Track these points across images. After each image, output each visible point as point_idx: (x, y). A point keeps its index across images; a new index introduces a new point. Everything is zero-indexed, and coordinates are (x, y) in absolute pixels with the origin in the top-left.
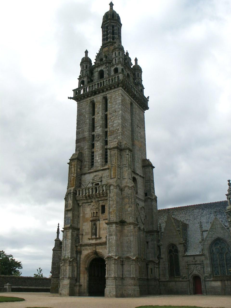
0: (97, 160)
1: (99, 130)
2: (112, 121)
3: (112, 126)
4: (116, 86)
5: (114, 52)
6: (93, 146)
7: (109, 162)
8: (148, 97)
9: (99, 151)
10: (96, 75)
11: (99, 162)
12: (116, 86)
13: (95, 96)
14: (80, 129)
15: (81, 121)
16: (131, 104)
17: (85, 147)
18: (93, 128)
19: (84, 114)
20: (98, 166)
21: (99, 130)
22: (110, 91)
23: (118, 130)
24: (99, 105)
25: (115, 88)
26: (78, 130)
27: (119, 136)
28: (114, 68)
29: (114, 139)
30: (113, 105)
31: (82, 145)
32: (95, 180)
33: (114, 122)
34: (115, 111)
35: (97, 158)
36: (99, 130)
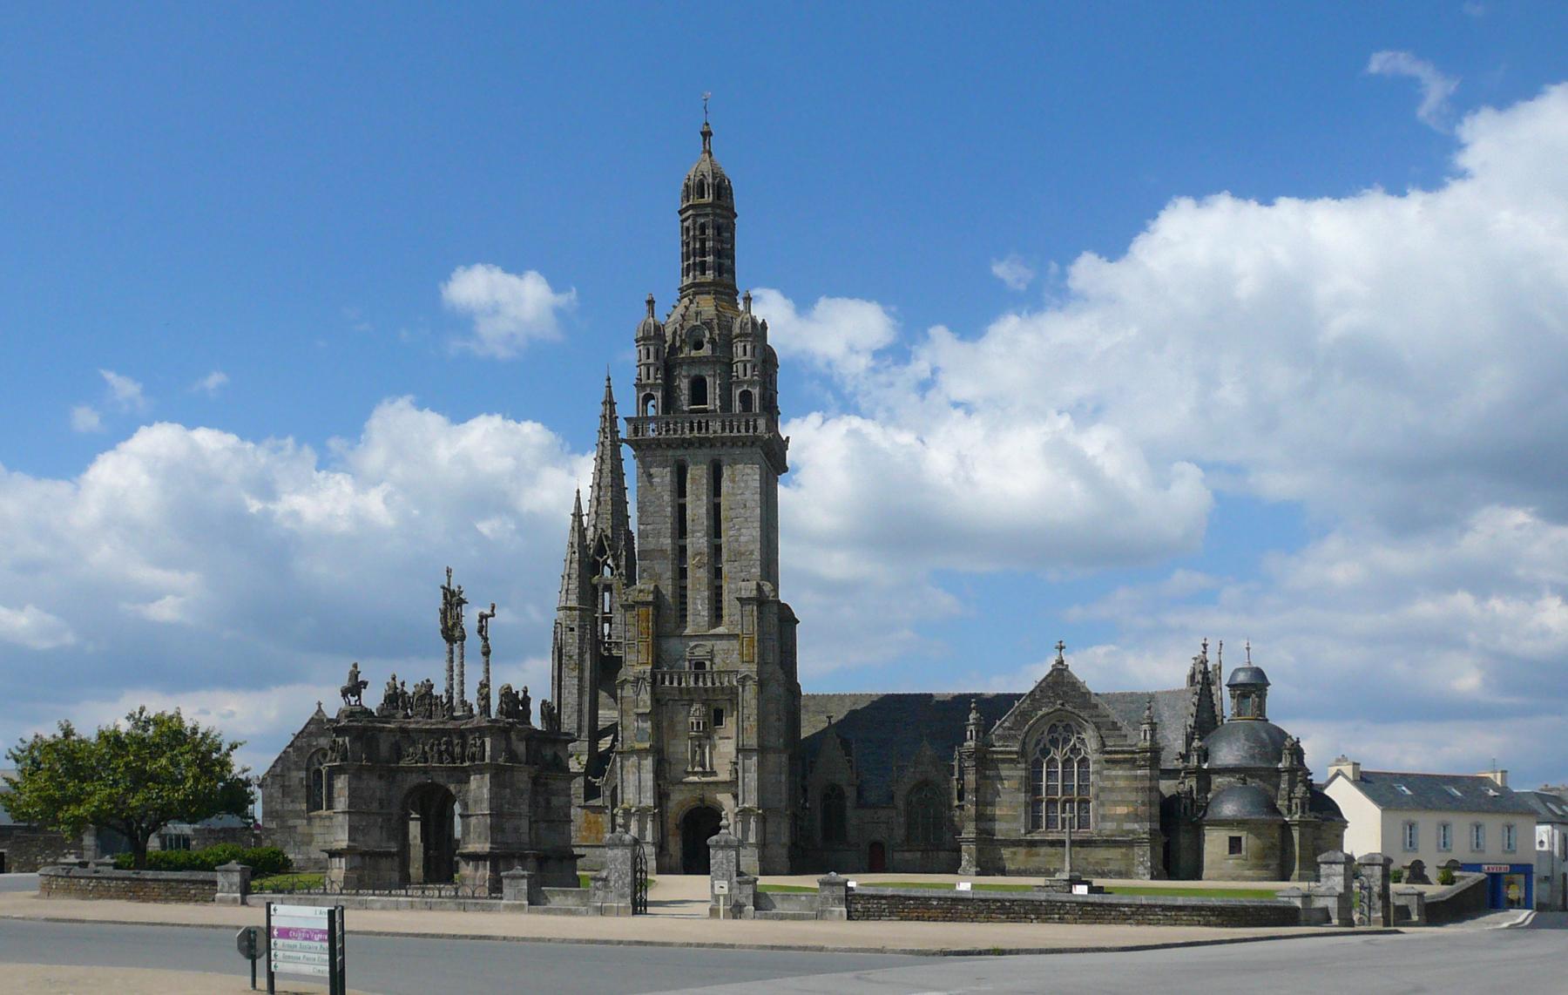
0: (699, 611)
1: (697, 541)
2: (737, 527)
3: (737, 541)
4: (748, 444)
5: (743, 344)
6: (682, 573)
7: (726, 619)
8: (788, 438)
9: (704, 591)
10: (684, 385)
11: (703, 616)
12: (748, 444)
13: (691, 451)
14: (649, 527)
15: (650, 506)
16: (767, 474)
17: (665, 573)
18: (681, 529)
19: (659, 489)
20: (702, 624)
21: (701, 541)
22: (731, 450)
23: (752, 553)
24: (701, 477)
25: (744, 444)
26: (642, 527)
27: (755, 568)
28: (741, 390)
29: (742, 571)
30: (739, 488)
31: (657, 567)
32: (696, 654)
33: (742, 530)
34: (745, 505)
35: (700, 608)
36: (697, 541)
